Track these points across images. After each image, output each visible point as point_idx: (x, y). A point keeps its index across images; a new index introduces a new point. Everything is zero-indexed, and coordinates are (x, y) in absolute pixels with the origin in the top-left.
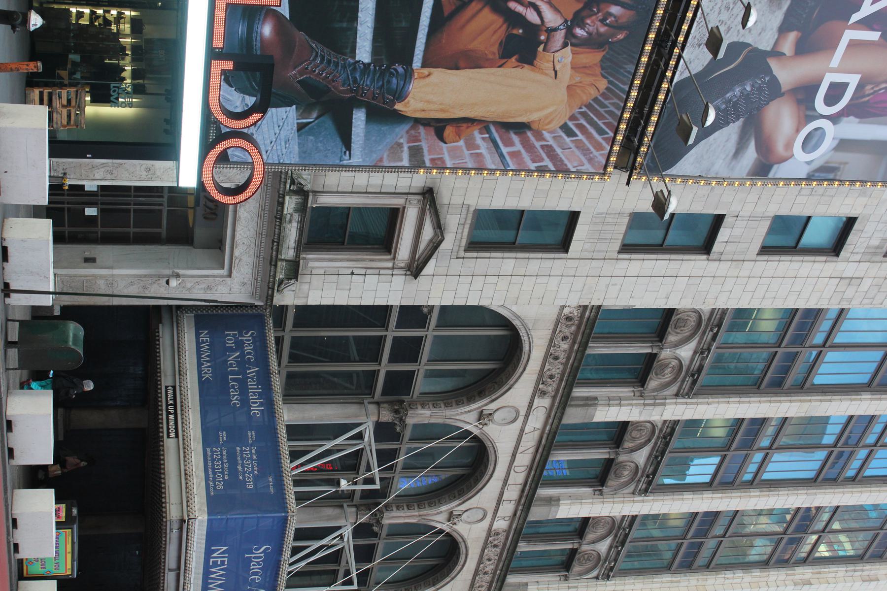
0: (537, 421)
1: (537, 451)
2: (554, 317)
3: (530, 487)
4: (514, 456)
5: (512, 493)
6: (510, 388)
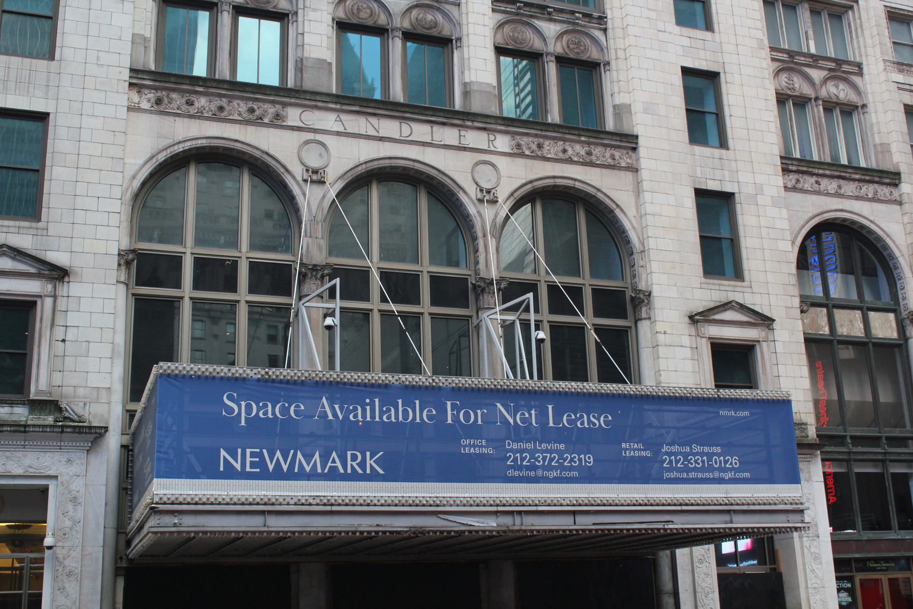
0: (327, 120)
1: (375, 115)
2: (155, 118)
3: (432, 116)
4: (381, 139)
5: (449, 135)
6: (267, 154)
